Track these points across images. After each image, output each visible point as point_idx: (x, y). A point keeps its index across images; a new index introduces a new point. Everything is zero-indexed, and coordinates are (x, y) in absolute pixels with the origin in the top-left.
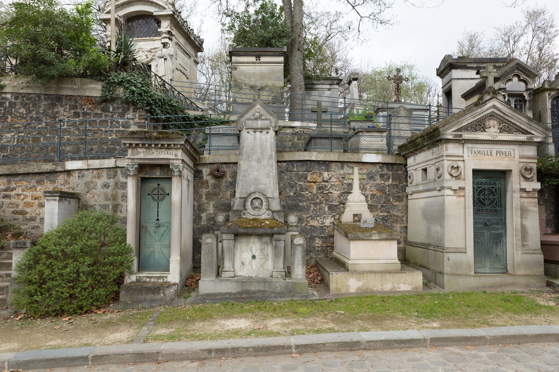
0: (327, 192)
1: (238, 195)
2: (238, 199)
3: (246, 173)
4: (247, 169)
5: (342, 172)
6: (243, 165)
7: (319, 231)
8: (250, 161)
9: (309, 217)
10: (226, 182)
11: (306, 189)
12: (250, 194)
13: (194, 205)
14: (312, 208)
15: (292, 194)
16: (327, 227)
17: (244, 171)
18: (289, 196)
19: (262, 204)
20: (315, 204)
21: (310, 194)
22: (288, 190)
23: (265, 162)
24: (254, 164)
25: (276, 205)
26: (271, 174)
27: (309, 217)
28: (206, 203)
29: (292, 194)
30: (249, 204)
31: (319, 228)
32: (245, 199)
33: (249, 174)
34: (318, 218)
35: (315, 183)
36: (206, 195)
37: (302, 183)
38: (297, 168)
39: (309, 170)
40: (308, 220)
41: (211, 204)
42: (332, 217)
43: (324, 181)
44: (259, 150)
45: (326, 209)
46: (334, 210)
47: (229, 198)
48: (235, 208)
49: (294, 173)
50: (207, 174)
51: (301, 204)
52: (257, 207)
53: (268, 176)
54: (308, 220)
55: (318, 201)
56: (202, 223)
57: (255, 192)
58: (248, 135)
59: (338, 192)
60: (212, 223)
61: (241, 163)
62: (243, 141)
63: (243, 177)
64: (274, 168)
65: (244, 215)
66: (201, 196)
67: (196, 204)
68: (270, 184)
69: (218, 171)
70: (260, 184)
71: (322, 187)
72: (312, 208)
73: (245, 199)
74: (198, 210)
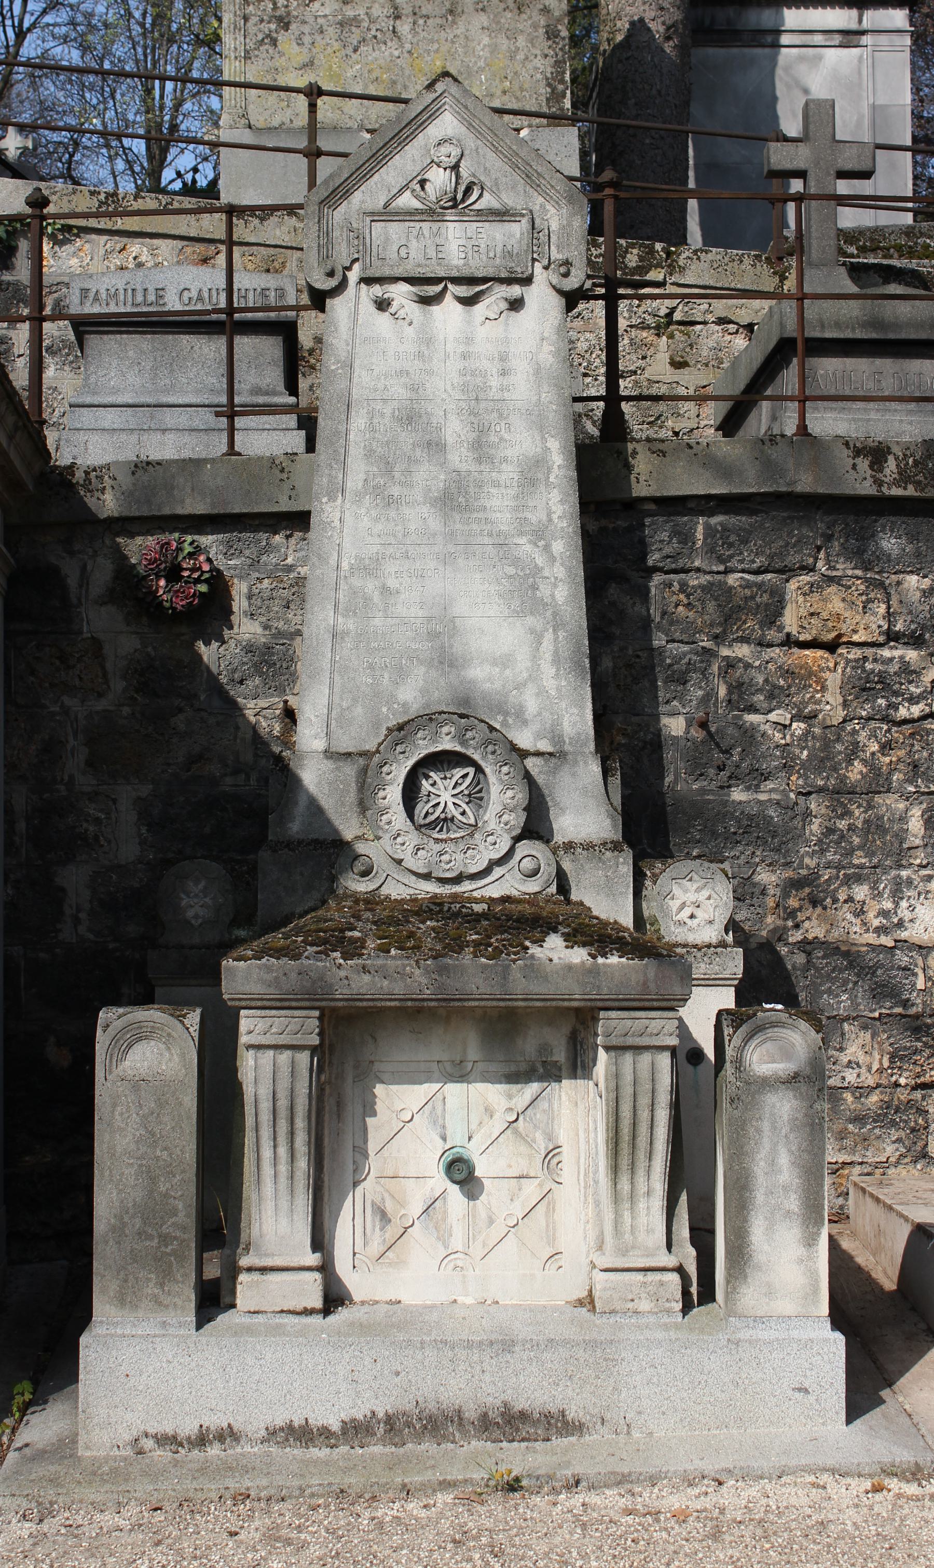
0: (916, 710)
3: (371, 586)
4: (378, 560)
8: (390, 502)
11: (775, 695)
14: (815, 827)
20: (840, 794)
21: (798, 727)
33: (385, 590)
34: (861, 892)
35: (831, 647)
37: (743, 651)
39: (793, 559)
51: (738, 795)
55: (856, 772)
71: (882, 678)
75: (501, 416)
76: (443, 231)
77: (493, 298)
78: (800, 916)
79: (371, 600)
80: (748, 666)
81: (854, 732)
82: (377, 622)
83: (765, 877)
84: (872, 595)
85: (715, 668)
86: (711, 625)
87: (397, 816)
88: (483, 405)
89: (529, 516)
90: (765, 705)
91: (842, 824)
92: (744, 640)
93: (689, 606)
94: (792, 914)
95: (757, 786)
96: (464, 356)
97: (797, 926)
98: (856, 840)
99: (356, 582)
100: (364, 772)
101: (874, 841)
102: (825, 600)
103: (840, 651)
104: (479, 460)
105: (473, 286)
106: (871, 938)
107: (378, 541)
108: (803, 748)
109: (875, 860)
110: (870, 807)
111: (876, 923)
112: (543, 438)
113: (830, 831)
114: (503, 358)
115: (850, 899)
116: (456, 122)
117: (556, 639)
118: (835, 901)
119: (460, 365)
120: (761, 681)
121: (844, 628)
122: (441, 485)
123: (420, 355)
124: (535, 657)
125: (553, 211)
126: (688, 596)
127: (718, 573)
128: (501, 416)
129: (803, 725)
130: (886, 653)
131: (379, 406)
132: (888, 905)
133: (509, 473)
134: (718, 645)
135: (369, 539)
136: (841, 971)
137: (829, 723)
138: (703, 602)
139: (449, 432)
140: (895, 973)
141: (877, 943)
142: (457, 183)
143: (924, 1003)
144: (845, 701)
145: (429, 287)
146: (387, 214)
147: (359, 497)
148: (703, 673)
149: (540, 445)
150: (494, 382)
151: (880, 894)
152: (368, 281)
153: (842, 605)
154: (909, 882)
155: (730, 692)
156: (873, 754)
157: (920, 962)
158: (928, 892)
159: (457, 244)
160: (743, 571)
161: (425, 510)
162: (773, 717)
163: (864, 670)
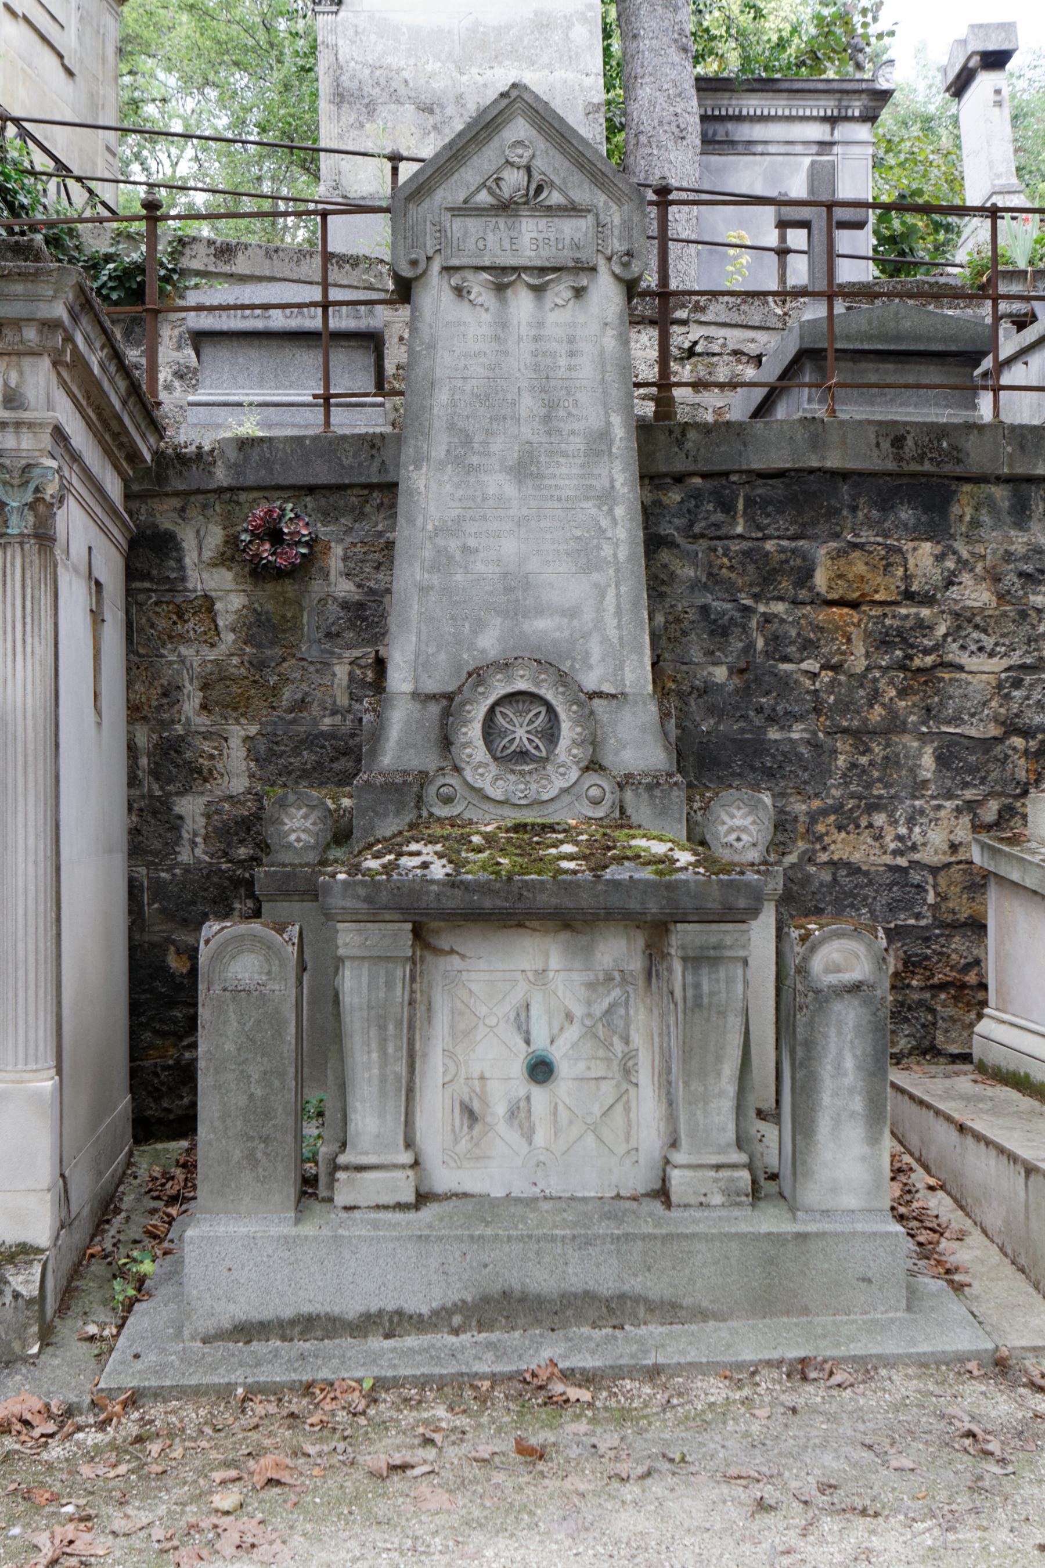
0: (929, 660)
1: (400, 680)
3: (453, 544)
4: (459, 520)
5: (1019, 542)
6: (431, 493)
7: (883, 899)
8: (471, 469)
9: (824, 812)
11: (808, 647)
13: (132, 749)
14: (841, 761)
15: (720, 674)
16: (935, 870)
17: (437, 531)
18: (707, 689)
19: (551, 734)
21: (827, 676)
22: (696, 655)
23: (565, 475)
24: (497, 483)
25: (638, 743)
26: (607, 550)
27: (824, 812)
28: (207, 736)
29: (720, 674)
31: (887, 878)
32: (448, 706)
33: (465, 549)
34: (880, 819)
35: (854, 605)
36: (204, 687)
37: (779, 608)
38: (750, 519)
40: (821, 828)
41: (235, 742)
42: (958, 810)
43: (909, 596)
44: (528, 403)
45: (928, 761)
46: (973, 770)
47: (343, 700)
49: (735, 546)
50: (207, 555)
51: (774, 734)
52: (522, 755)
53: (586, 559)
54: (821, 828)
56: (185, 856)
58: (462, 312)
59: (997, 664)
60: (243, 852)
61: (421, 484)
62: (432, 347)
63: (434, 568)
64: (620, 511)
65: (448, 800)
66: (171, 693)
67: (142, 740)
68: (600, 609)
69: (276, 536)
70: (540, 611)
72: (841, 761)
73: (448, 706)
74: (155, 773)
75: (569, 393)
76: (517, 225)
77: (562, 287)
78: (827, 840)
79: (453, 557)
80: (782, 621)
81: (875, 680)
82: (459, 577)
83: (799, 807)
84: (891, 560)
85: (754, 624)
86: (751, 585)
87: (479, 752)
88: (553, 383)
89: (594, 483)
90: (798, 655)
91: (864, 760)
92: (781, 599)
93: (731, 568)
94: (820, 838)
95: (790, 726)
96: (536, 339)
97: (824, 849)
98: (876, 774)
99: (441, 542)
100: (446, 713)
101: (891, 775)
102: (851, 564)
103: (864, 608)
104: (549, 433)
105: (541, 276)
106: (888, 859)
107: (459, 505)
108: (831, 693)
109: (892, 791)
110: (888, 745)
111: (892, 846)
112: (606, 412)
113: (854, 765)
114: (571, 340)
115: (870, 826)
116: (527, 126)
117: (618, 595)
118: (858, 826)
119: (533, 347)
120: (793, 633)
121: (867, 589)
122: (516, 455)
123: (497, 338)
124: (600, 609)
125: (615, 207)
126: (730, 560)
127: (758, 539)
128: (569, 393)
129: (830, 674)
130: (903, 611)
131: (459, 383)
132: (903, 831)
133: (577, 444)
134: (756, 602)
135: (452, 504)
136: (862, 888)
137: (853, 671)
138: (743, 565)
139: (523, 407)
140: (908, 889)
141: (893, 863)
142: (529, 182)
143: (934, 916)
144: (867, 652)
145: (503, 277)
146: (465, 210)
147: (441, 466)
148: (744, 628)
149: (602, 417)
150: (563, 362)
151: (896, 822)
152: (448, 269)
153: (865, 568)
154: (922, 812)
155: (767, 644)
156: (891, 699)
157: (931, 880)
158: (938, 820)
159: (530, 239)
160: (779, 538)
161: (501, 477)
162: (804, 666)
163: (884, 626)
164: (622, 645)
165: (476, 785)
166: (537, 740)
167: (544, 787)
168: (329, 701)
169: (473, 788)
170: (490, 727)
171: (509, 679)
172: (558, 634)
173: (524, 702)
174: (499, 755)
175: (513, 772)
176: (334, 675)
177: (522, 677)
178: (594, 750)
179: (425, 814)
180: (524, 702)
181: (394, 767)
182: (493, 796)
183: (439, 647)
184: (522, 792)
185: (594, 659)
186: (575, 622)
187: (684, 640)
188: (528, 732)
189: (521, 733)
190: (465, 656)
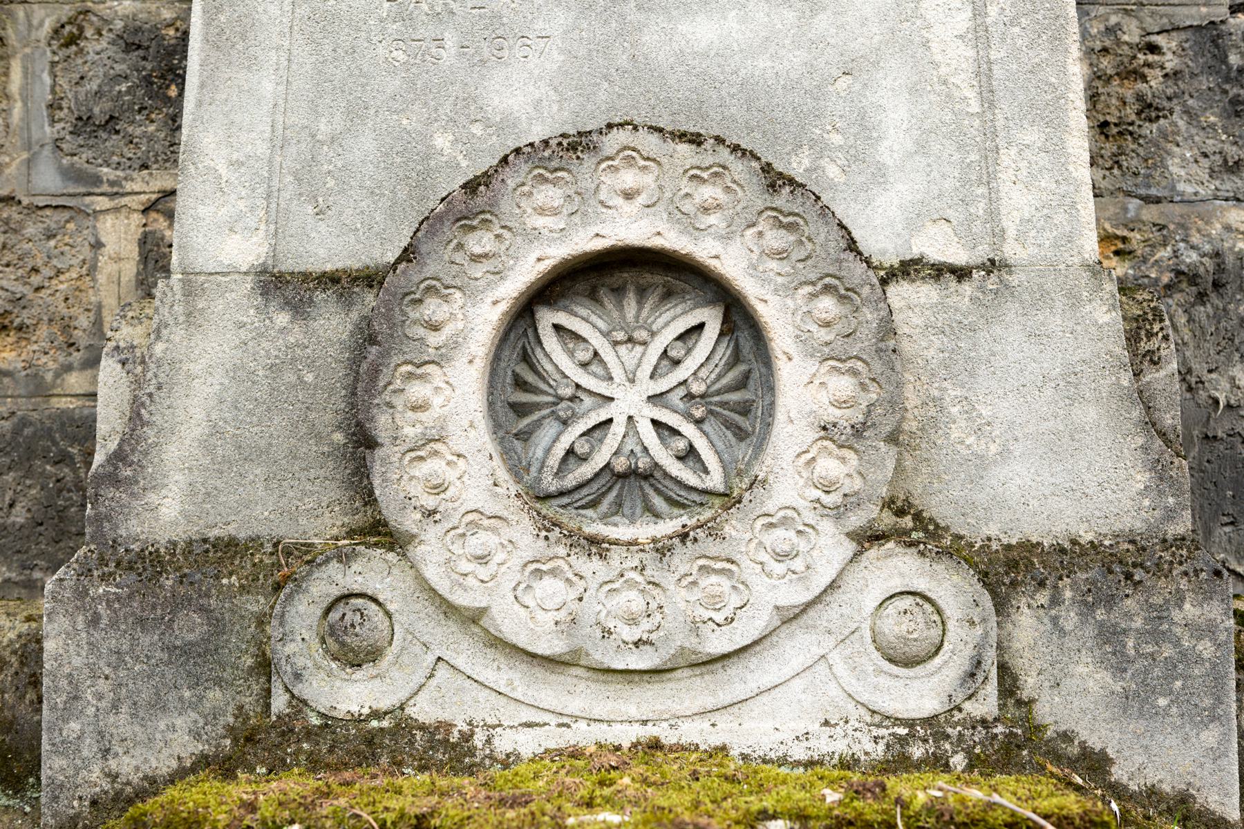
1: (222, 232)
2: (235, 306)
10: (69, 37)
12: (475, 200)
30: (449, 396)
48: (166, 510)
52: (633, 483)
57: (578, 144)
73: (371, 305)
164: (988, 98)
165: (461, 599)
166: (689, 430)
167: (715, 601)
168: (84, 321)
169: (448, 609)
170: (520, 384)
171: (582, 205)
172: (763, 63)
173: (642, 293)
174: (550, 484)
175: (596, 545)
176: (98, 245)
177: (629, 195)
178: (899, 468)
179: (279, 703)
180: (642, 293)
181: (194, 531)
182: (522, 641)
183: (356, 113)
184: (632, 621)
185: (893, 143)
186: (822, 22)
187: (1150, 130)
188: (655, 399)
189: (630, 402)
190: (442, 141)
